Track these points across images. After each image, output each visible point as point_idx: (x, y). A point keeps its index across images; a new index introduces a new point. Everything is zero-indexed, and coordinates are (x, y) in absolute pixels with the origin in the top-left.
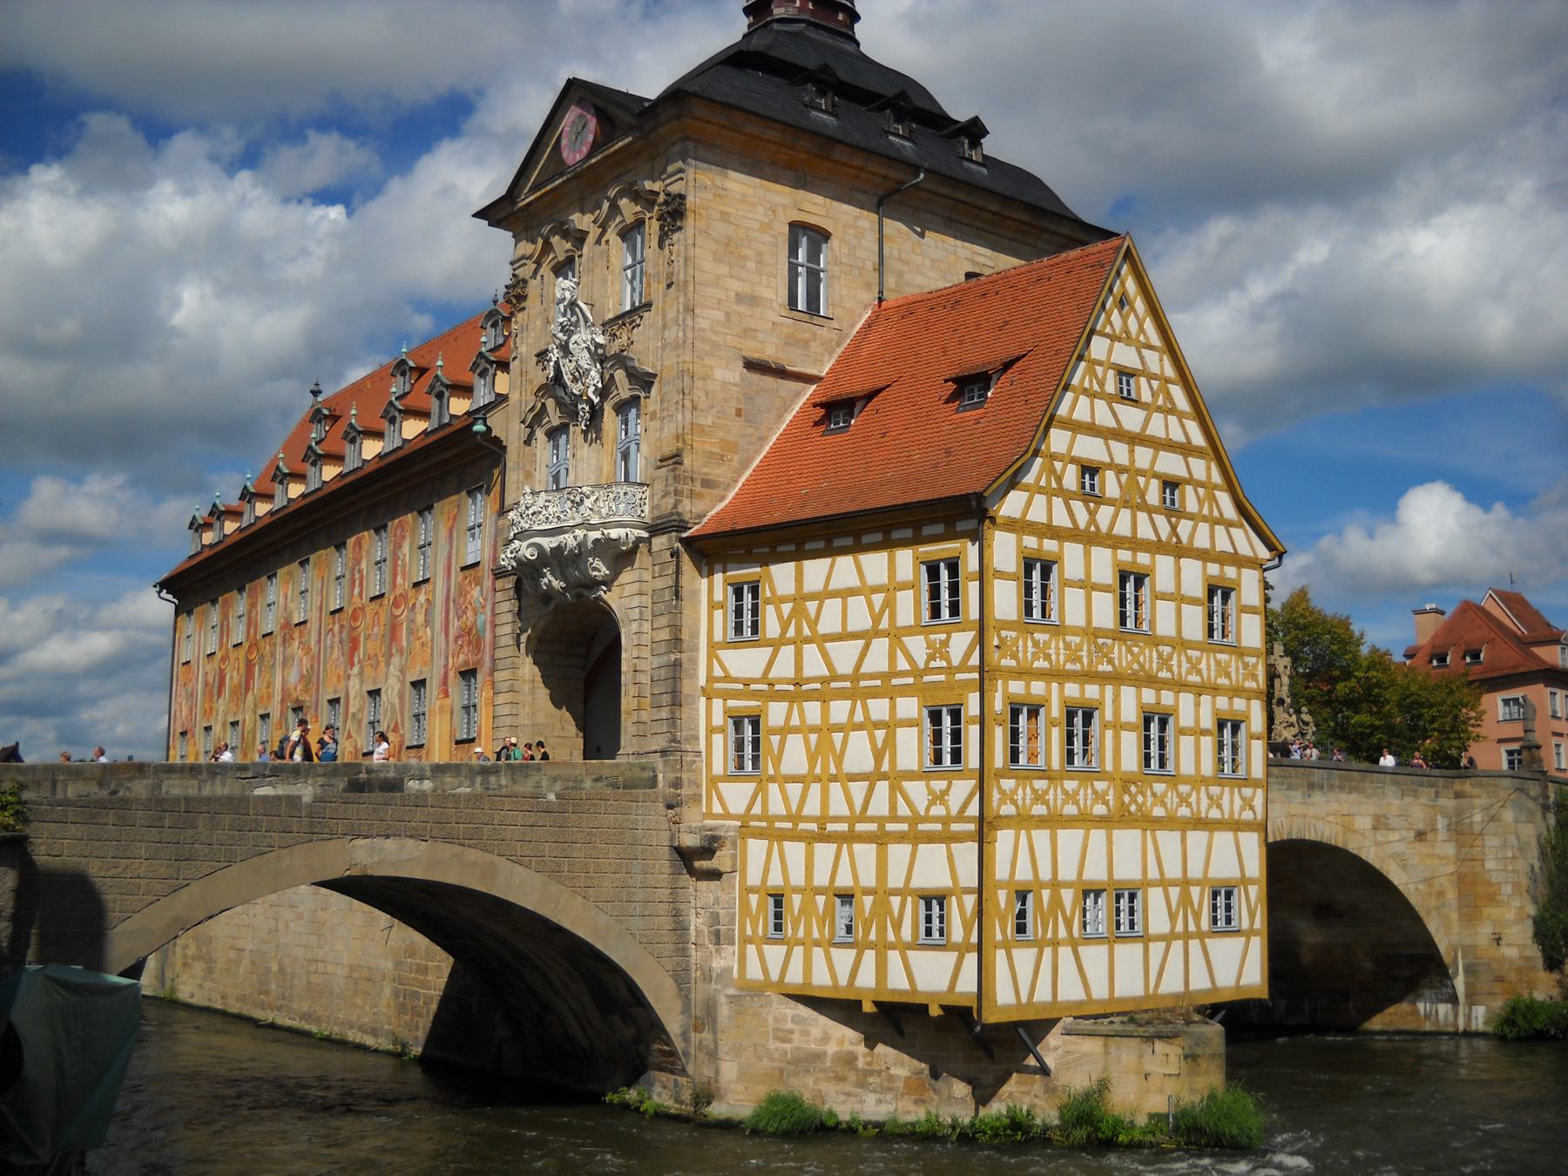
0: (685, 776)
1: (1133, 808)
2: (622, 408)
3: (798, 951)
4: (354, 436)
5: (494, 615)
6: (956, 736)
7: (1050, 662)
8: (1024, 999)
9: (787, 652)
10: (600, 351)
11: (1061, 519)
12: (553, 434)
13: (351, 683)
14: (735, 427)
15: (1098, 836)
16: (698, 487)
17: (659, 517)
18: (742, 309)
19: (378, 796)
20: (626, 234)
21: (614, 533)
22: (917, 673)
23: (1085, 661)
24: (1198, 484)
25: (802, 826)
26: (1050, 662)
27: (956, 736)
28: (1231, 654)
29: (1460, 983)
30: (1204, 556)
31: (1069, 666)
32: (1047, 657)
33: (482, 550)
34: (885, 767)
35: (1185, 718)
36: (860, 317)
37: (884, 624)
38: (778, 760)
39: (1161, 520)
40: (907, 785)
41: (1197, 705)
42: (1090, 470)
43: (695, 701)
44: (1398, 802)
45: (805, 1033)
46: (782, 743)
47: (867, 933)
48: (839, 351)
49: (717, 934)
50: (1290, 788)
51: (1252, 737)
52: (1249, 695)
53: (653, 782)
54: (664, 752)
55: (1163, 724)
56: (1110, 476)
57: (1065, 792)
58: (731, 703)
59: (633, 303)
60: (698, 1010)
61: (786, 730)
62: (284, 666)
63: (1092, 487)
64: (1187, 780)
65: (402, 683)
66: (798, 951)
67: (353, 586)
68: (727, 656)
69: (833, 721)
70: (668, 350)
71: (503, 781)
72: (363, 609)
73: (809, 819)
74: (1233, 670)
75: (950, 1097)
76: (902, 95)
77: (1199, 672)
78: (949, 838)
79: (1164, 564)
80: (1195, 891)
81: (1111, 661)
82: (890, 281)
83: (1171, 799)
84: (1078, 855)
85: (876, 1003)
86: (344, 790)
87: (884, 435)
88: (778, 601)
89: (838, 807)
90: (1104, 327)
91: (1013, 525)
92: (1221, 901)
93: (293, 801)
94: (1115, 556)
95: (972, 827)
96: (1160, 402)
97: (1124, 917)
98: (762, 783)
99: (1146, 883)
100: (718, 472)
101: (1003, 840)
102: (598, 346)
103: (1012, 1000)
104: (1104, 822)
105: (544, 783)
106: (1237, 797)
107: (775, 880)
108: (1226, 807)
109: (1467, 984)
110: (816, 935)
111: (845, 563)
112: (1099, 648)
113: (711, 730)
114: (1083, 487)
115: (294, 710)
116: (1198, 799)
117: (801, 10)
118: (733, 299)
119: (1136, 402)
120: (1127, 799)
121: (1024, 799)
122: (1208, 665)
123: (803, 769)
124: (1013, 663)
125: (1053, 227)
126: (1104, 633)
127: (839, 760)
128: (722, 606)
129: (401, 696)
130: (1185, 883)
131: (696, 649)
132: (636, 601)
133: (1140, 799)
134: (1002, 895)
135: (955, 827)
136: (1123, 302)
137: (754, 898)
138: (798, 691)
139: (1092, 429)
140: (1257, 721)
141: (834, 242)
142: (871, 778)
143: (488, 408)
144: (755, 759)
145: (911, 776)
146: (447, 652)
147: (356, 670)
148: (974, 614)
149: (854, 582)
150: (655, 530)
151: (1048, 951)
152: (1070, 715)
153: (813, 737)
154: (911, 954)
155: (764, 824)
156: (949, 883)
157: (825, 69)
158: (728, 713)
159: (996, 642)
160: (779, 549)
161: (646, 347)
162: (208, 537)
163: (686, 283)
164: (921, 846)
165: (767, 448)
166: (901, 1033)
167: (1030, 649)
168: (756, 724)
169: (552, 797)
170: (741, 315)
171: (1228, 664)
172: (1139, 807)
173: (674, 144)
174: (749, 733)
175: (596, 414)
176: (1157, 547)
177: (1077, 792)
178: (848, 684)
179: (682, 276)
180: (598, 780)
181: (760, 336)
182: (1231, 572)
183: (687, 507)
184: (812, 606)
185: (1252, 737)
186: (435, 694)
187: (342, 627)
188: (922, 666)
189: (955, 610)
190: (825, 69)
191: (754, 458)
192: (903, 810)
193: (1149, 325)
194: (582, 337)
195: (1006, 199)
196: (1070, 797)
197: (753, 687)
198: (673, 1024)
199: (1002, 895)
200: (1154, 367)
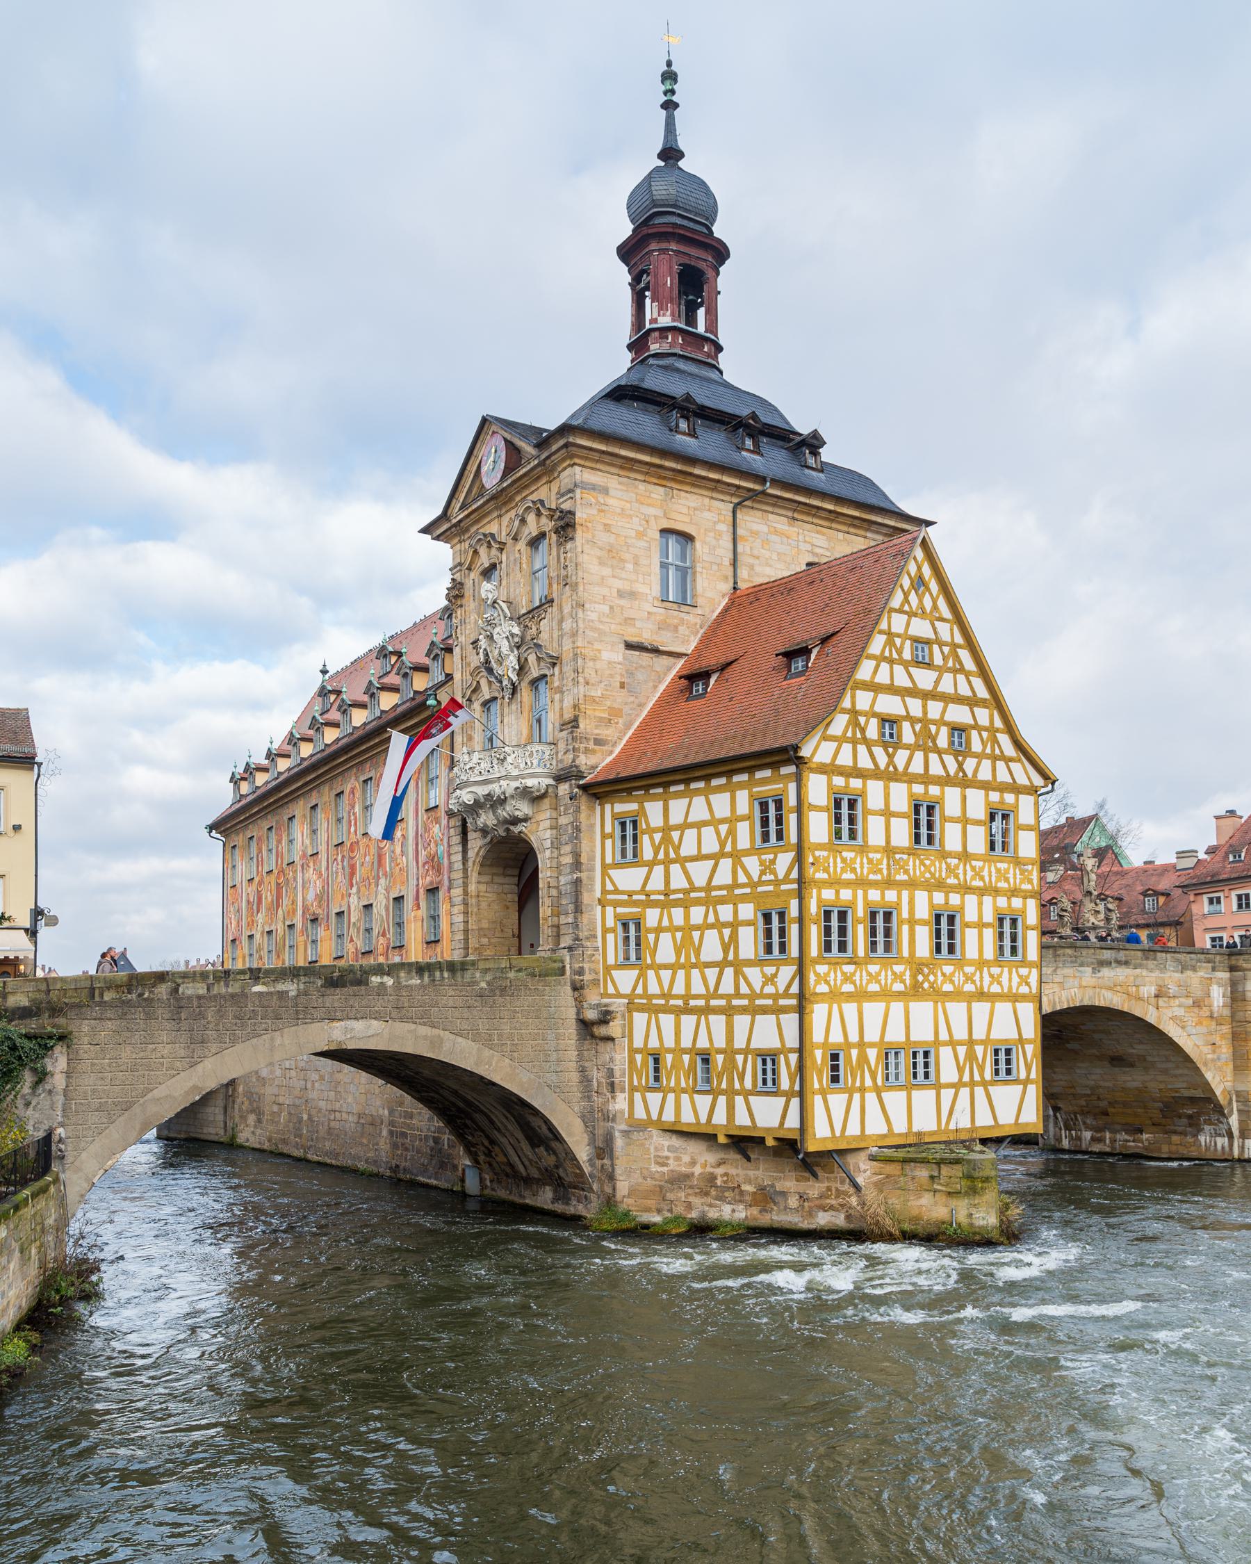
0: (586, 966)
1: (926, 985)
2: (534, 683)
3: (671, 1096)
6: (782, 933)
7: (856, 874)
8: (838, 1134)
9: (659, 870)
11: (865, 762)
14: (620, 698)
15: (897, 1008)
18: (623, 602)
21: (530, 782)
22: (753, 885)
23: (885, 872)
25: (672, 1002)
26: (856, 874)
27: (782, 933)
29: (1234, 1121)
31: (872, 877)
32: (853, 870)
34: (731, 957)
35: (971, 915)
36: (720, 603)
37: (728, 848)
38: (654, 953)
39: (950, 760)
40: (746, 970)
41: (980, 904)
44: (1178, 975)
47: (720, 1083)
48: (702, 631)
52: (1026, 896)
53: (562, 971)
54: (570, 949)
57: (869, 974)
58: (619, 910)
61: (659, 930)
64: (971, 963)
66: (671, 1096)
71: (446, 975)
73: (678, 997)
74: (1011, 876)
75: (786, 1208)
77: (982, 878)
78: (778, 1010)
79: (952, 797)
80: (979, 1050)
81: (906, 872)
82: (743, 573)
83: (958, 978)
85: (728, 1136)
87: (731, 700)
88: (651, 831)
89: (698, 988)
91: (823, 769)
92: (1002, 1056)
93: (282, 995)
94: (910, 789)
95: (794, 1002)
96: (950, 664)
97: (920, 1070)
99: (937, 1043)
100: (608, 732)
101: (818, 1013)
102: (513, 635)
103: (827, 1133)
104: (899, 995)
105: (478, 975)
107: (654, 1043)
109: (1241, 1122)
110: (683, 1084)
111: (699, 801)
113: (605, 931)
114: (883, 735)
116: (981, 977)
118: (615, 594)
120: (920, 978)
121: (835, 980)
122: (990, 872)
123: (672, 959)
124: (825, 876)
125: (879, 520)
126: (901, 851)
127: (698, 954)
128: (611, 836)
130: (971, 1043)
131: (592, 870)
134: (818, 1054)
137: (639, 1057)
138: (667, 900)
140: (1032, 914)
141: (698, 544)
144: (638, 952)
145: (749, 963)
148: (793, 839)
149: (706, 816)
150: (559, 779)
151: (857, 1096)
152: (873, 915)
153: (679, 935)
154: (751, 1098)
155: (645, 1001)
156: (778, 1045)
158: (616, 916)
159: (811, 860)
160: (652, 791)
163: (577, 584)
165: (645, 713)
166: (749, 1159)
167: (840, 865)
168: (638, 925)
169: (483, 985)
170: (622, 607)
171: (1007, 871)
172: (932, 986)
177: (878, 974)
178: (703, 894)
180: (520, 970)
181: (638, 624)
182: (1010, 798)
183: (583, 761)
184: (675, 835)
188: (756, 879)
189: (780, 836)
192: (744, 989)
195: (839, 500)
196: (873, 978)
197: (635, 897)
199: (818, 1054)
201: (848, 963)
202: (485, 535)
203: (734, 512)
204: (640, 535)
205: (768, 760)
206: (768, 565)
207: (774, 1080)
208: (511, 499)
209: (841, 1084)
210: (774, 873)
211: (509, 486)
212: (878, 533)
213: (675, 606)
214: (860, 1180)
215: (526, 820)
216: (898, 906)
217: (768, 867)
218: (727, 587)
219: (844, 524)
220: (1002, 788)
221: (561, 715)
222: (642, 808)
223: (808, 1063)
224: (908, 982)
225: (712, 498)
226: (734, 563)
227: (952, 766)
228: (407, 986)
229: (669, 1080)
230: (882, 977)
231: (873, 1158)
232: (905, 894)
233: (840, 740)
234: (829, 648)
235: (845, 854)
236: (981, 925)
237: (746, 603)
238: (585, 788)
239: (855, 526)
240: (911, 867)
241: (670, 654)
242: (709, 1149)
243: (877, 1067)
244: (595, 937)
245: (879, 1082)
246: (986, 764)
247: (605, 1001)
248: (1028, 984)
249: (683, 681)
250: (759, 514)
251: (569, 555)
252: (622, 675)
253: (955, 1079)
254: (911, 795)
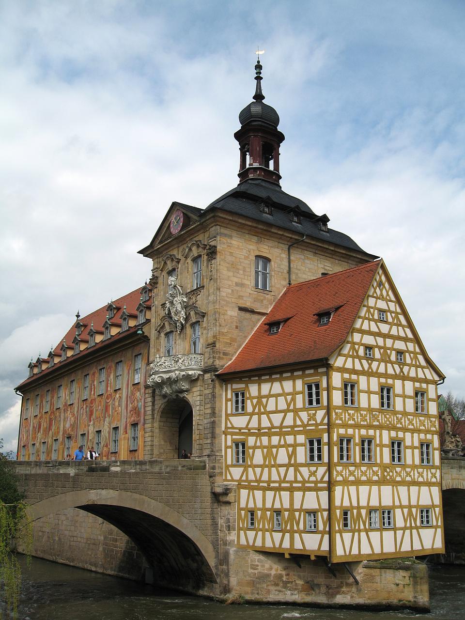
0: (217, 465)
1: (388, 477)
2: (193, 325)
3: (260, 533)
4: (92, 334)
5: (145, 403)
6: (319, 450)
7: (355, 422)
9: (255, 418)
10: (185, 304)
11: (358, 367)
12: (167, 334)
13: (90, 428)
14: (236, 332)
15: (375, 488)
16: (221, 355)
17: (207, 367)
18: (238, 288)
19: (99, 473)
20: (195, 260)
21: (190, 373)
22: (304, 426)
23: (368, 421)
24: (410, 352)
25: (261, 484)
27: (319, 450)
28: (425, 417)
30: (414, 380)
31: (362, 423)
32: (354, 420)
33: (141, 378)
34: (293, 462)
35: (408, 442)
36: (282, 290)
37: (292, 407)
39: (396, 366)
41: (412, 437)
42: (369, 348)
43: (221, 436)
45: (263, 566)
46: (253, 452)
47: (286, 526)
49: (229, 526)
50: (452, 468)
51: (435, 449)
53: (204, 467)
54: (209, 456)
55: (399, 445)
56: (376, 350)
57: (362, 471)
59: (197, 286)
60: (221, 557)
61: (254, 448)
62: (64, 420)
63: (370, 355)
64: (409, 466)
65: (110, 428)
66: (260, 533)
67: (92, 391)
68: (232, 419)
69: (272, 444)
70: (210, 304)
72: (95, 399)
76: (297, 207)
77: (413, 425)
78: (316, 489)
79: (398, 383)
80: (414, 510)
81: (378, 421)
82: (293, 277)
83: (403, 474)
84: (367, 496)
85: (290, 554)
86: (87, 471)
89: (275, 477)
90: (373, 294)
91: (339, 370)
92: (425, 514)
93: (67, 475)
94: (379, 380)
95: (326, 485)
97: (386, 520)
98: (246, 468)
99: (394, 507)
101: (338, 490)
103: (343, 554)
106: (429, 473)
107: (251, 505)
108: (425, 477)
110: (267, 527)
112: (373, 416)
113: (227, 447)
114: (366, 354)
115: (67, 438)
117: (259, 175)
118: (234, 285)
119: (386, 322)
120: (386, 474)
122: (416, 421)
123: (262, 462)
124: (341, 422)
125: (354, 255)
128: (231, 400)
129: (109, 433)
130: (410, 507)
132: (198, 398)
133: (391, 474)
134: (338, 512)
135: (319, 485)
136: (380, 284)
137: (243, 512)
138: (259, 432)
139: (369, 333)
140: (436, 443)
141: (272, 263)
142: (287, 466)
143: (144, 324)
145: (302, 465)
146: (127, 416)
147: (92, 423)
148: (325, 403)
149: (280, 391)
150: (205, 371)
151: (356, 534)
152: (363, 442)
153: (265, 450)
155: (247, 484)
157: (269, 198)
158: (233, 441)
160: (252, 379)
161: (201, 302)
162: (36, 371)
163: (217, 279)
164: (306, 492)
165: (247, 340)
166: (300, 567)
167: (347, 417)
171: (424, 421)
172: (391, 477)
173: (212, 227)
174: (241, 447)
175: (183, 327)
176: (395, 377)
178: (278, 430)
179: (215, 276)
180: (184, 466)
181: (244, 298)
182: (424, 386)
183: (218, 363)
184: (264, 400)
185: (435, 449)
186: (122, 432)
187: (87, 406)
189: (318, 402)
190: (269, 198)
191: (243, 344)
192: (299, 478)
193: (390, 293)
194: (178, 299)
195: (336, 245)
198: (212, 562)
199: (338, 512)
200: (392, 308)
201: (352, 466)
202: (171, 255)
203: (289, 249)
204: (246, 258)
205: (312, 365)
206: (304, 273)
207: (315, 525)
208: (185, 239)
209: (349, 528)
210: (315, 420)
211: (182, 234)
212: (353, 261)
213: (262, 291)
214: (358, 578)
215: (186, 391)
216: (375, 436)
217: (312, 417)
218: (285, 283)
219: (339, 256)
220: (421, 381)
221: (207, 341)
222: (247, 386)
223: (333, 517)
224: (380, 475)
225: (279, 242)
226: (289, 272)
227: (398, 370)
228: (129, 473)
229: (259, 525)
230: (368, 473)
231: (366, 567)
232: (378, 432)
233: (347, 356)
234: (339, 312)
235: (349, 411)
236: (413, 448)
237: (295, 291)
238: (218, 376)
239: (343, 257)
240: (380, 419)
241: (259, 313)
242: (280, 561)
243: (366, 519)
244: (221, 450)
245: (367, 527)
246: (413, 369)
247: (226, 483)
248: (435, 477)
249: (266, 326)
250: (300, 250)
251: (213, 265)
252: (237, 322)
253: (403, 525)
254: (379, 383)
